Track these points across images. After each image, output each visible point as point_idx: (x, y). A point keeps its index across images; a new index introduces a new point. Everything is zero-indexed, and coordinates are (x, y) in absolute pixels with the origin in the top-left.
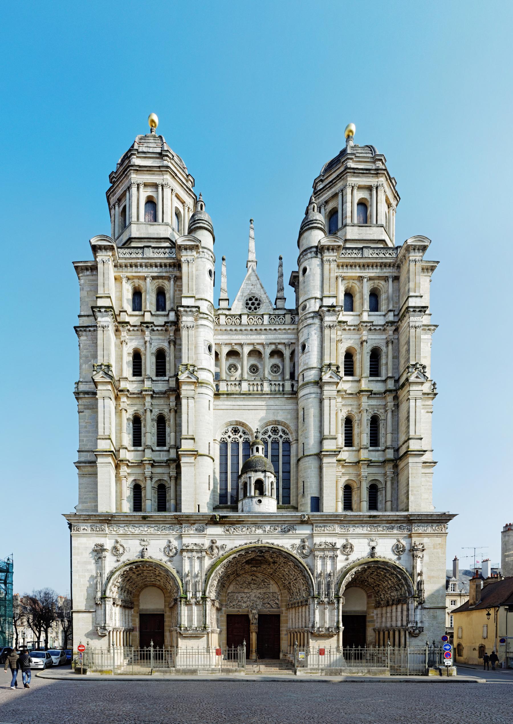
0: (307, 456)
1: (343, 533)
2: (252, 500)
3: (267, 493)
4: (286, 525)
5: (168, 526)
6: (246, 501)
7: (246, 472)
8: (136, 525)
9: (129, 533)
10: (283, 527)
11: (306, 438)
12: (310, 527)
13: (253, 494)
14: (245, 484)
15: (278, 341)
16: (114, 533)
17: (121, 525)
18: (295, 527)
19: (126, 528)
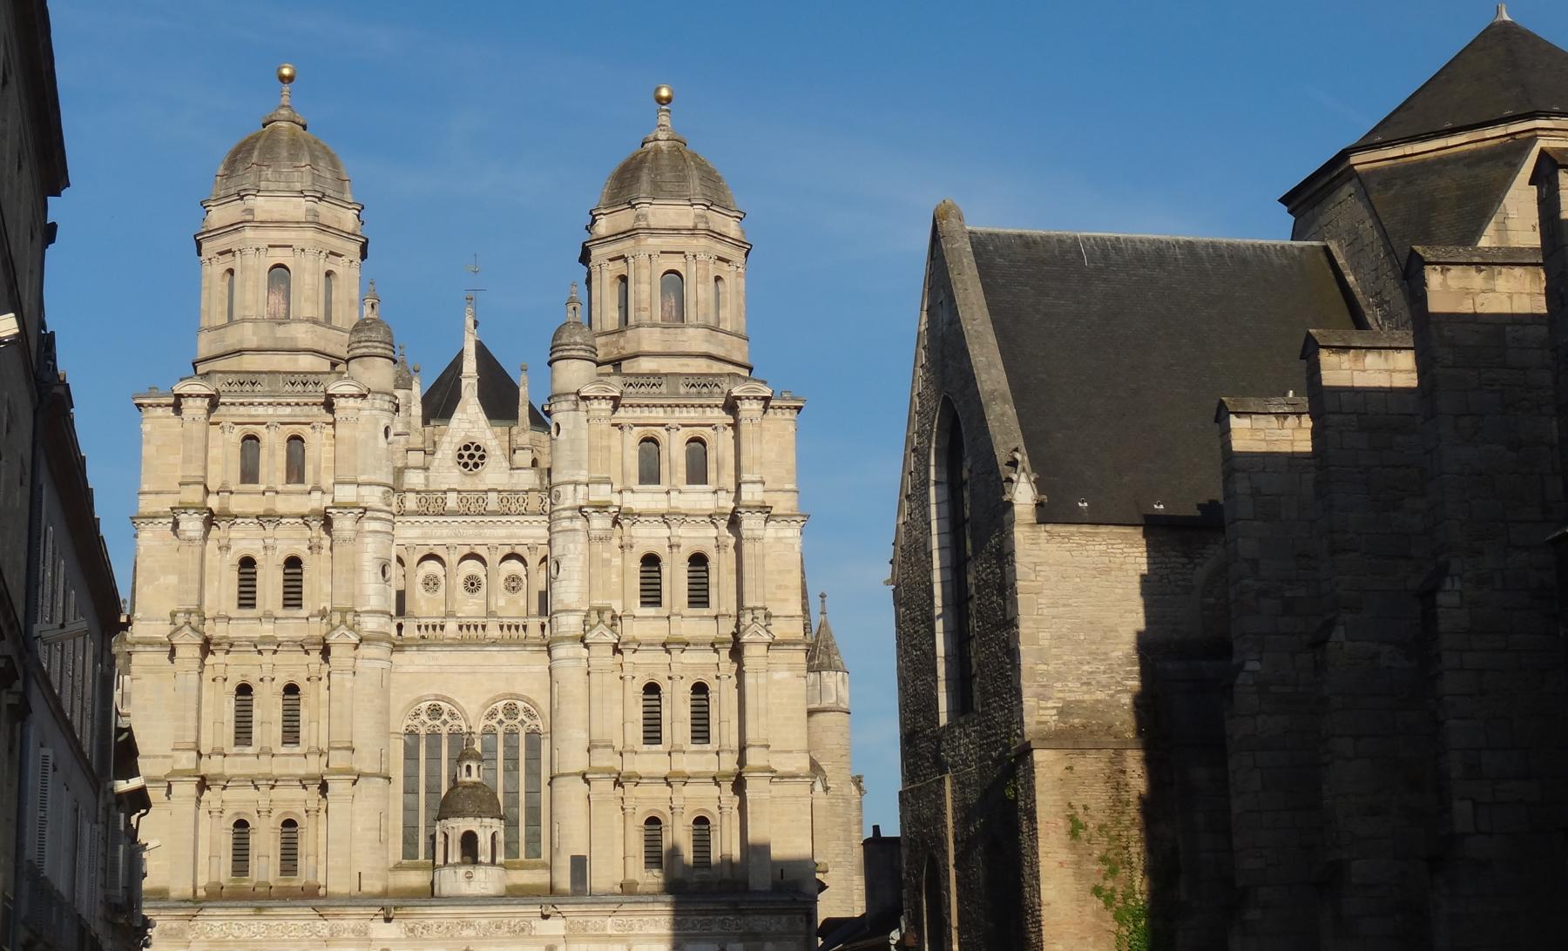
0: (563, 775)
3: (484, 857)
5: (301, 923)
6: (446, 872)
12: (562, 922)
15: (515, 541)
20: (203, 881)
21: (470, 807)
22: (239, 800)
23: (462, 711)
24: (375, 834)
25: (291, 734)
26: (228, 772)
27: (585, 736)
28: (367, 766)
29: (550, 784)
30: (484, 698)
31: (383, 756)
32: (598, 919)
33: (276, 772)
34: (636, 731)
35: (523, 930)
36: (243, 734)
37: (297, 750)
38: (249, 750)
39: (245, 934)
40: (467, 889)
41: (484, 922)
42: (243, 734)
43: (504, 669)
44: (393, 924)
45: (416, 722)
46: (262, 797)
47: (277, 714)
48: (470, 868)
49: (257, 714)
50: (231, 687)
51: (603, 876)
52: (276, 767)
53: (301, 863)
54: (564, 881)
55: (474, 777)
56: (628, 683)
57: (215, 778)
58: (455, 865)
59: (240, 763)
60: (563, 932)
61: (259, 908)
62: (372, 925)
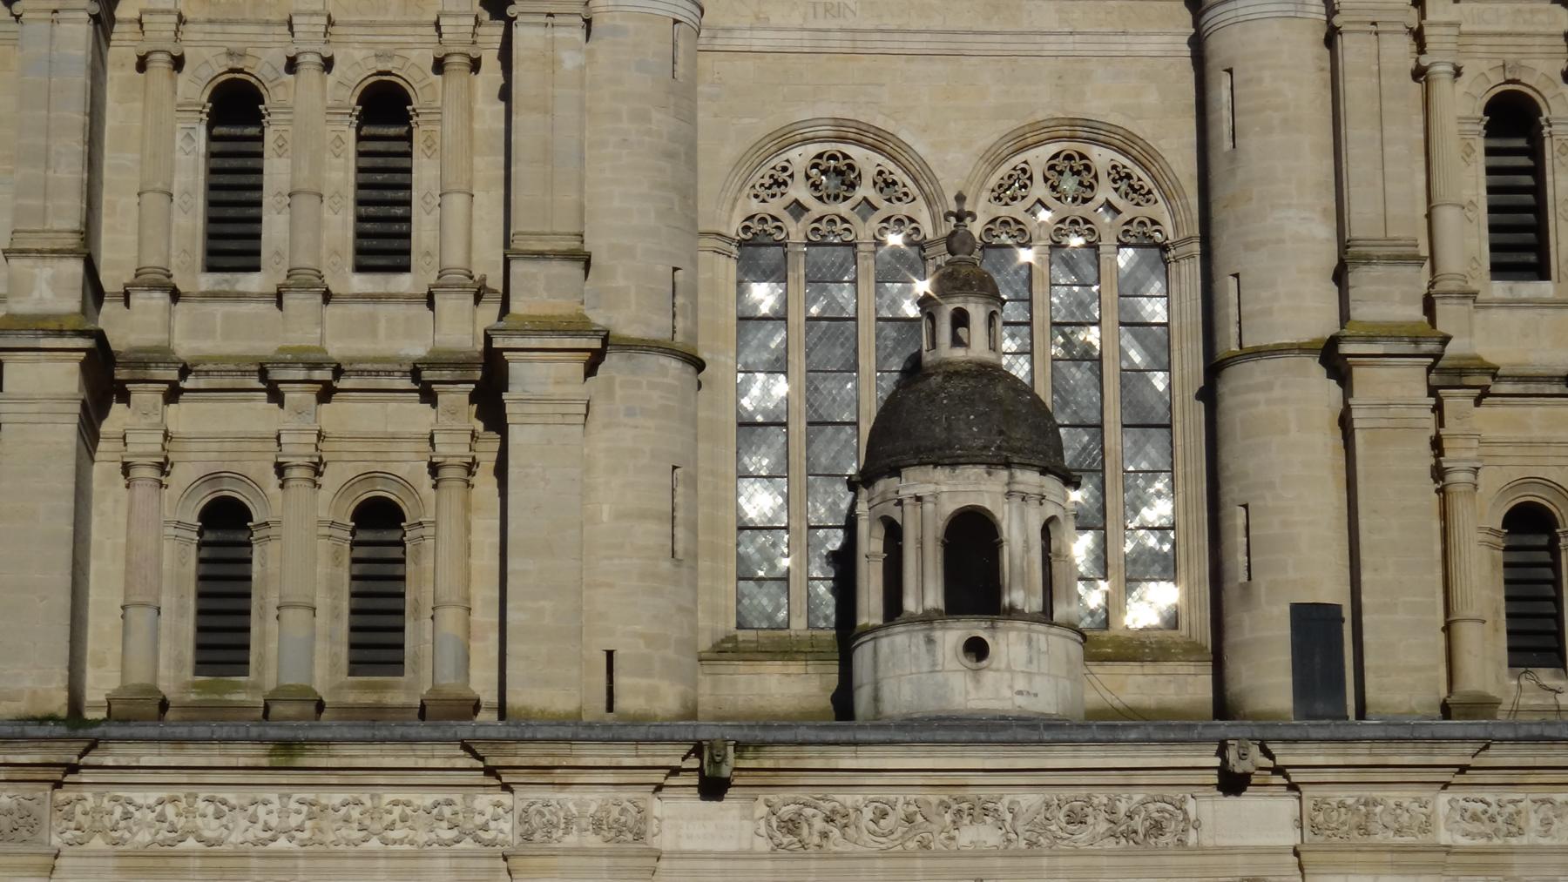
0: (1259, 353)
1: (1482, 842)
2: (930, 641)
4: (1138, 795)
5: (427, 799)
6: (900, 641)
7: (895, 472)
8: (231, 796)
9: (191, 843)
10: (1123, 807)
11: (1247, 247)
12: (1286, 805)
13: (934, 598)
14: (893, 533)
16: (98, 843)
17: (139, 796)
18: (1191, 806)
19: (170, 810)
20: (99, 687)
21: (971, 433)
22: (220, 434)
23: (921, 173)
24: (652, 533)
25: (383, 242)
26: (185, 347)
27: (1324, 231)
28: (625, 324)
29: (1209, 395)
30: (989, 135)
31: (678, 290)
32: (1406, 796)
33: (336, 349)
34: (1467, 240)
35: (1157, 828)
36: (232, 238)
37: (402, 283)
38: (250, 282)
39: (239, 834)
40: (967, 692)
41: (1029, 800)
42: (232, 238)
43: (1052, 45)
44: (729, 809)
45: (775, 207)
46: (297, 421)
47: (341, 173)
48: (977, 628)
49: (276, 171)
50: (195, 88)
51: (1399, 665)
52: (339, 335)
53: (417, 635)
54: (1269, 679)
55: (978, 348)
56: (1443, 88)
57: (143, 361)
58: (928, 618)
59: (224, 323)
60: (1291, 838)
61: (287, 746)
62: (658, 807)
